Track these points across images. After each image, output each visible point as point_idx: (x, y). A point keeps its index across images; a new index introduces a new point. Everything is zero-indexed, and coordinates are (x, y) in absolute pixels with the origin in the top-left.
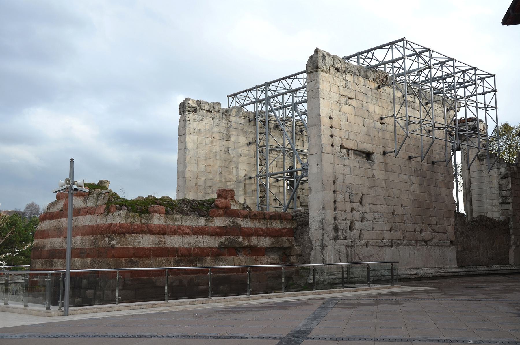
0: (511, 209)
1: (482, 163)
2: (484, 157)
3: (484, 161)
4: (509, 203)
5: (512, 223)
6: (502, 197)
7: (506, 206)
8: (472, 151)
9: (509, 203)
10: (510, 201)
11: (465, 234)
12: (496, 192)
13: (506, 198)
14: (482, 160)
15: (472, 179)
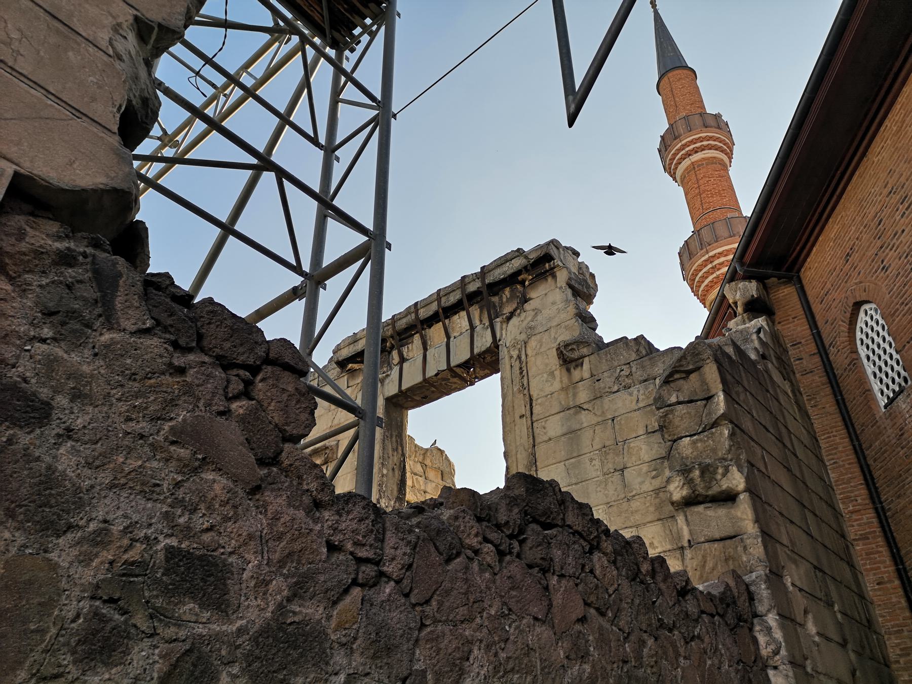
0: (750, 527)
1: (576, 374)
2: (585, 351)
3: (586, 366)
4: (729, 498)
5: (772, 619)
6: (685, 471)
7: (715, 519)
8: (540, 342)
9: (729, 498)
10: (736, 480)
11: (254, 613)
12: (648, 486)
13: (707, 471)
14: (577, 362)
15: (540, 451)
